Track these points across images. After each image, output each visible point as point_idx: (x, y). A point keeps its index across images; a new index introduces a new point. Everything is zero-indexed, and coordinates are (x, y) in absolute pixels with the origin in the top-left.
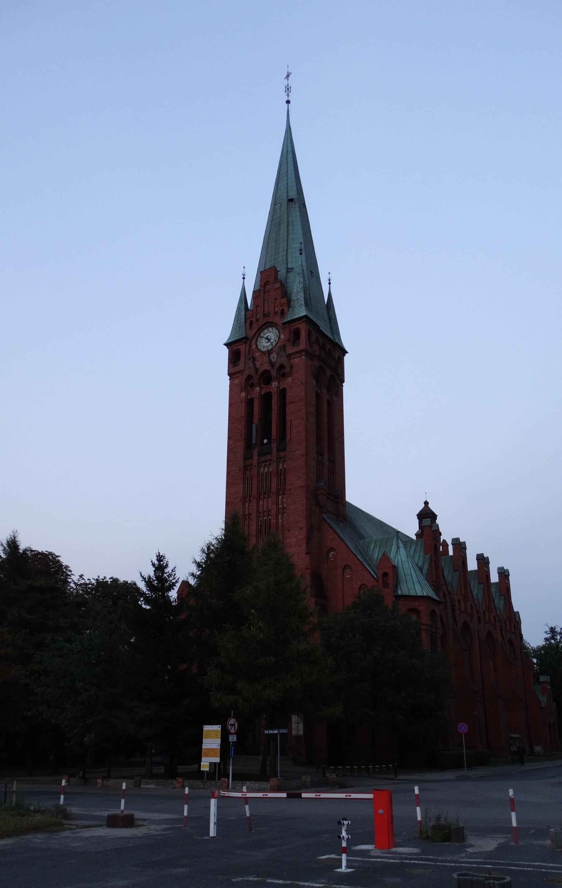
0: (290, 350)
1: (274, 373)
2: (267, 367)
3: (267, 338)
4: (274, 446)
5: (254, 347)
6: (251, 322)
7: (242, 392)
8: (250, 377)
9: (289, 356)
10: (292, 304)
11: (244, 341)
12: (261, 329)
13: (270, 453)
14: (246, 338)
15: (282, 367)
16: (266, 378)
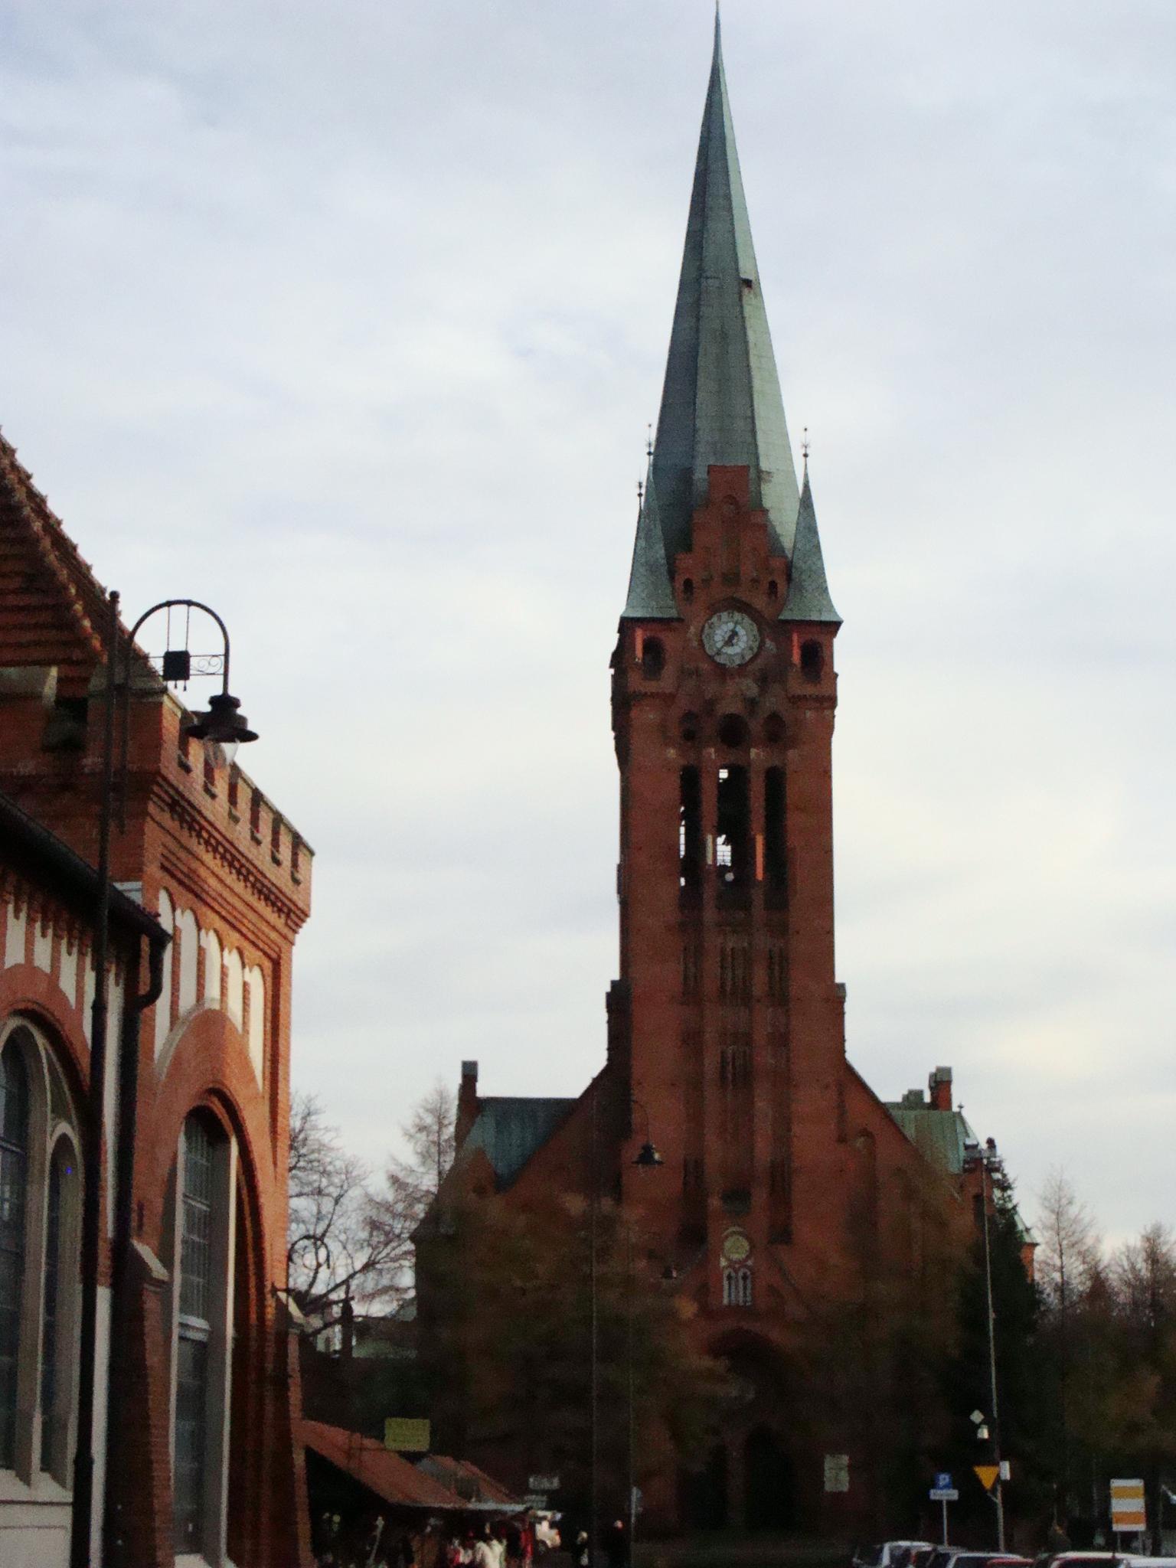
0: (797, 686)
1: (756, 726)
2: (731, 706)
3: (731, 638)
4: (758, 897)
5: (695, 644)
6: (688, 584)
7: (667, 745)
8: (689, 716)
9: (796, 700)
10: (795, 575)
11: (675, 624)
12: (714, 609)
13: (746, 906)
14: (680, 620)
15: (774, 719)
16: (733, 734)
